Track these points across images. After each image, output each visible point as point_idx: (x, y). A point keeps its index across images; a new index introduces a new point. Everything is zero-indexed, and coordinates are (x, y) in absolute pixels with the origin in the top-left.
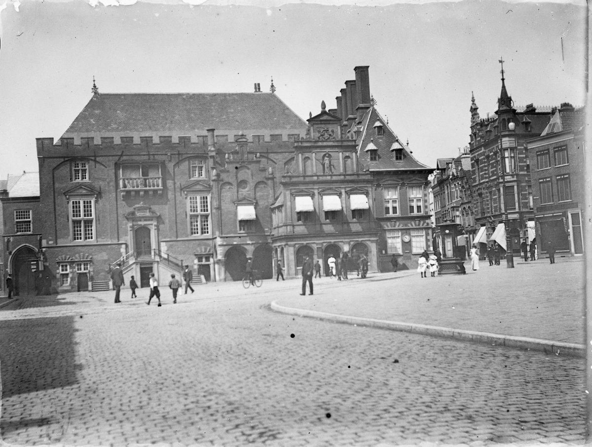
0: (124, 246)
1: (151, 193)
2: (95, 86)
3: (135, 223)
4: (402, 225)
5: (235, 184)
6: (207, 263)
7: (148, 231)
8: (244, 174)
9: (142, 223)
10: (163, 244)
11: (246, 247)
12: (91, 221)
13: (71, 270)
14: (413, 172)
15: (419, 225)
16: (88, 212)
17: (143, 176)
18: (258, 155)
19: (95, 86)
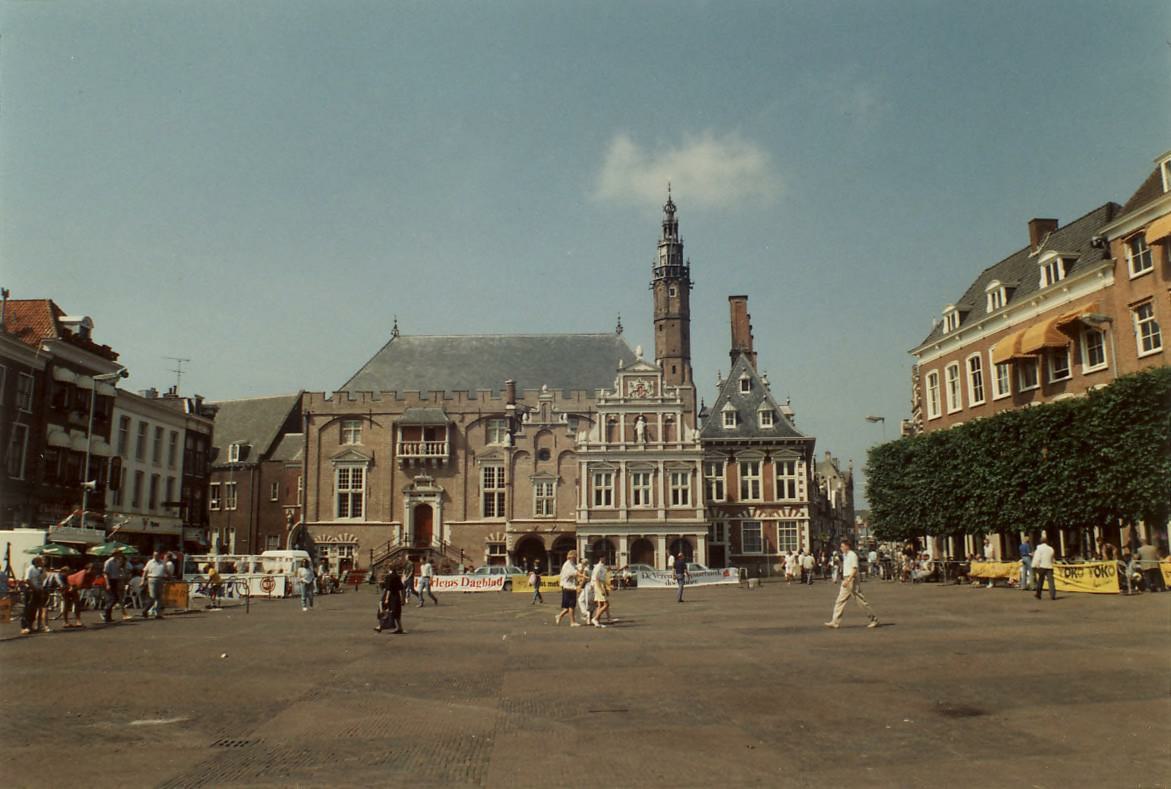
0: (397, 528)
1: (434, 461)
2: (396, 327)
3: (412, 499)
4: (764, 515)
5: (532, 452)
6: (502, 555)
7: (430, 509)
8: (545, 442)
9: (422, 499)
10: (447, 528)
11: (543, 536)
12: (361, 495)
13: (332, 555)
14: (780, 443)
15: (790, 515)
16: (357, 483)
17: (425, 440)
18: (565, 415)
19: (396, 327)
